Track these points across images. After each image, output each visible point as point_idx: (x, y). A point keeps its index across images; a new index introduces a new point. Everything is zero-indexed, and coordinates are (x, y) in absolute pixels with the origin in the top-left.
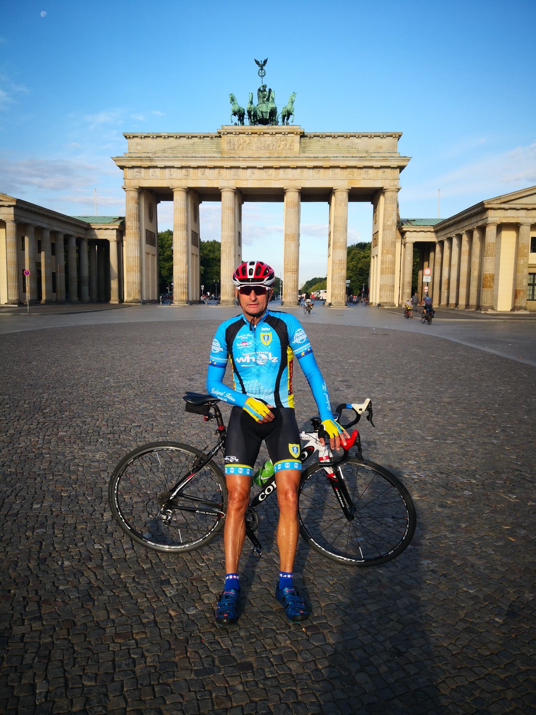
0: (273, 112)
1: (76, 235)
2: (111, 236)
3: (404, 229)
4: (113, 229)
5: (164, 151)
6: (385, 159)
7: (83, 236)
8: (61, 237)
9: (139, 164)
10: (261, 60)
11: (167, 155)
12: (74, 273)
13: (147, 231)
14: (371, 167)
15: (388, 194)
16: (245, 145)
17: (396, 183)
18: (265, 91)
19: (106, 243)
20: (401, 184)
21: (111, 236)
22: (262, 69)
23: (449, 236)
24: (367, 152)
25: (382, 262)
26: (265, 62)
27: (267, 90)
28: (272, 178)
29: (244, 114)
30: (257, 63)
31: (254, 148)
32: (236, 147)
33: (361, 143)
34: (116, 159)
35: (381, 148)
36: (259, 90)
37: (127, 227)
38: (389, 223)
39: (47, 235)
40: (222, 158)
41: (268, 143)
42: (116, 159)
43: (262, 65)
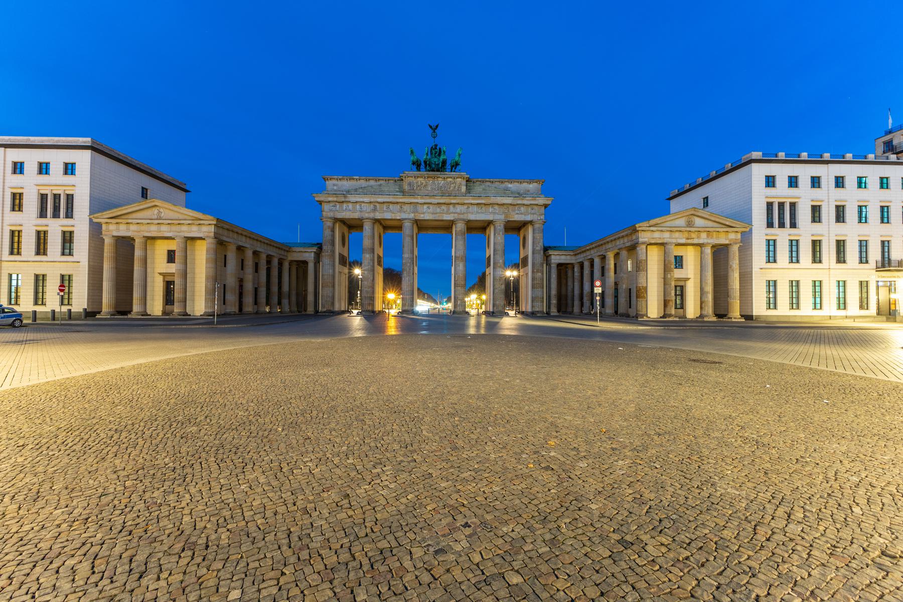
0: (444, 162)
12: (275, 289)
13: (340, 254)
19: (305, 263)
21: (309, 256)
25: (533, 279)
26: (437, 127)
30: (431, 127)
38: (538, 248)
43: (434, 129)
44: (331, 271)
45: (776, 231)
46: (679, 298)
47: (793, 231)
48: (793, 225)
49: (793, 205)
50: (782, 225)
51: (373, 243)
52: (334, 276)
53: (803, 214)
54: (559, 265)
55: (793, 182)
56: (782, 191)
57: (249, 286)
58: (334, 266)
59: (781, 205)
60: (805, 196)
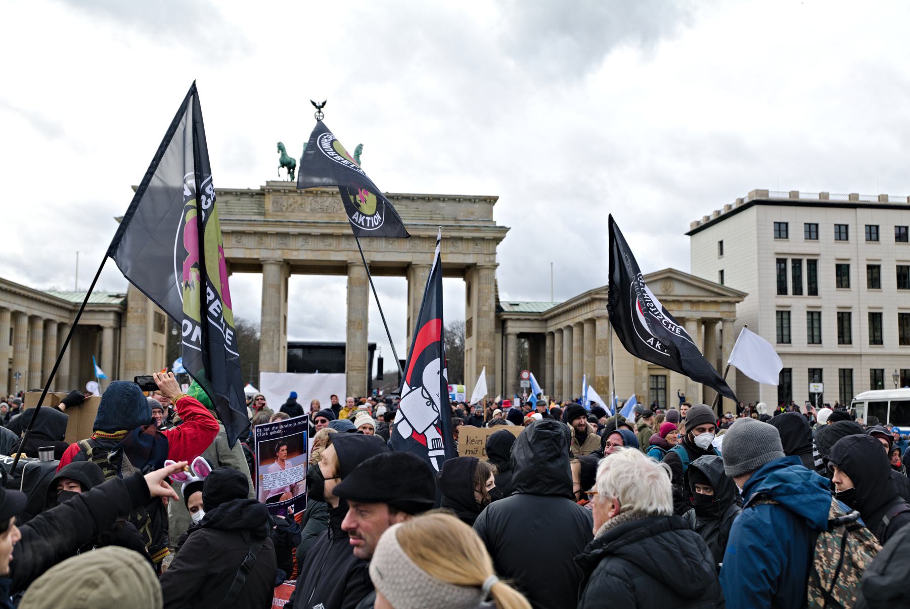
1: (59, 320)
2: (107, 321)
3: (505, 317)
4: (110, 312)
6: (478, 229)
8: (40, 324)
10: (319, 103)
14: (461, 239)
15: (484, 273)
16: (296, 206)
17: (492, 258)
19: (99, 329)
20: (499, 259)
22: (320, 112)
23: (559, 326)
24: (456, 220)
26: (324, 104)
28: (331, 248)
30: (314, 104)
31: (308, 210)
32: (284, 209)
33: (447, 209)
35: (472, 214)
37: (129, 309)
38: (485, 308)
39: (25, 321)
40: (266, 223)
41: (327, 204)
43: (319, 108)
44: (141, 343)
45: (789, 300)
46: (661, 393)
47: (813, 301)
48: (813, 291)
49: (813, 264)
50: (798, 291)
52: (145, 351)
53: (827, 276)
54: (521, 335)
55: (812, 231)
56: (797, 245)
57: (23, 368)
58: (145, 334)
59: (797, 263)
60: (828, 252)
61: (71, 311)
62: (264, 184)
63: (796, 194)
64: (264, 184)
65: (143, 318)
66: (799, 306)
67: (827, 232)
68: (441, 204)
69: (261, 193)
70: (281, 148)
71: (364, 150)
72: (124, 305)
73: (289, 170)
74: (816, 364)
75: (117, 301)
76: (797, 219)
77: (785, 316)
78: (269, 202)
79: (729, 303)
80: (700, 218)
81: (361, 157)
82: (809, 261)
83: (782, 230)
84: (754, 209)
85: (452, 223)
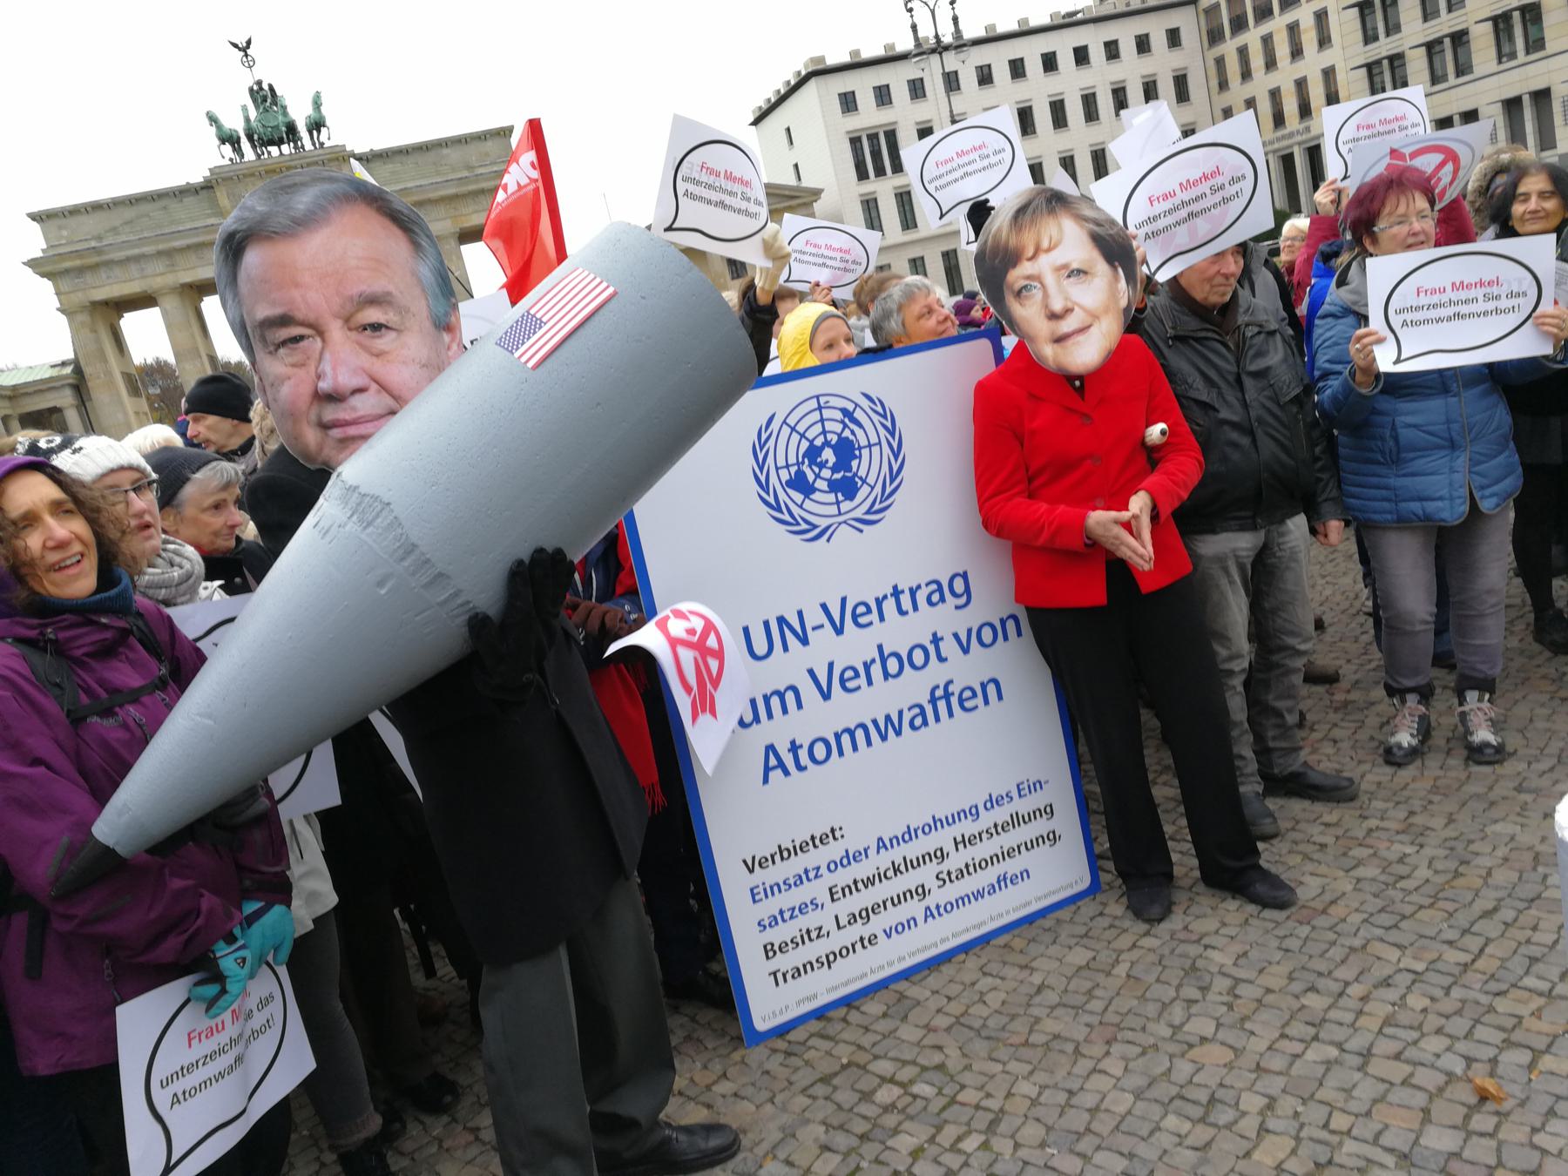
0: (291, 129)
2: (65, 399)
5: (114, 230)
7: (8, 412)
9: (78, 263)
10: (242, 42)
11: (124, 238)
18: (261, 89)
19: (56, 410)
24: (470, 168)
26: (249, 42)
27: (265, 87)
29: (238, 141)
30: (235, 46)
33: (453, 155)
34: (33, 264)
35: (487, 154)
36: (251, 90)
42: (33, 264)
43: (245, 49)
44: (120, 416)
45: (874, 186)
47: (899, 181)
48: (898, 168)
49: (891, 136)
50: (880, 172)
51: (193, 336)
55: (883, 95)
56: (869, 116)
58: (121, 403)
60: (905, 115)
61: (10, 398)
62: (208, 174)
63: (856, 53)
64: (208, 174)
65: (111, 383)
66: (884, 189)
67: (900, 92)
68: (445, 151)
69: (207, 187)
70: (213, 119)
71: (324, 100)
72: (78, 371)
73: (233, 145)
74: (915, 253)
75: (68, 370)
76: (863, 85)
77: (872, 205)
78: (222, 197)
79: (805, 204)
80: (761, 102)
81: (323, 109)
82: (886, 133)
83: (848, 102)
84: (812, 83)
85: (465, 174)
